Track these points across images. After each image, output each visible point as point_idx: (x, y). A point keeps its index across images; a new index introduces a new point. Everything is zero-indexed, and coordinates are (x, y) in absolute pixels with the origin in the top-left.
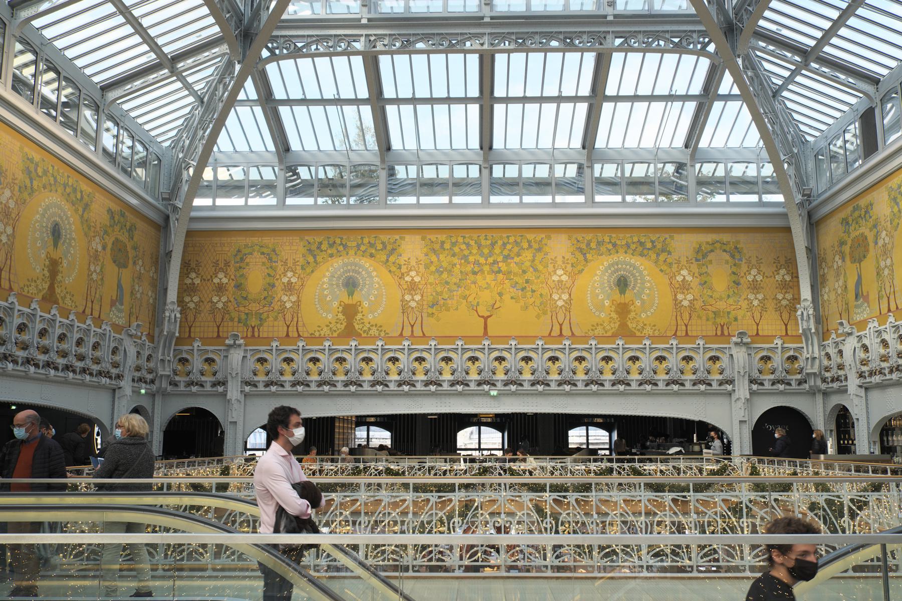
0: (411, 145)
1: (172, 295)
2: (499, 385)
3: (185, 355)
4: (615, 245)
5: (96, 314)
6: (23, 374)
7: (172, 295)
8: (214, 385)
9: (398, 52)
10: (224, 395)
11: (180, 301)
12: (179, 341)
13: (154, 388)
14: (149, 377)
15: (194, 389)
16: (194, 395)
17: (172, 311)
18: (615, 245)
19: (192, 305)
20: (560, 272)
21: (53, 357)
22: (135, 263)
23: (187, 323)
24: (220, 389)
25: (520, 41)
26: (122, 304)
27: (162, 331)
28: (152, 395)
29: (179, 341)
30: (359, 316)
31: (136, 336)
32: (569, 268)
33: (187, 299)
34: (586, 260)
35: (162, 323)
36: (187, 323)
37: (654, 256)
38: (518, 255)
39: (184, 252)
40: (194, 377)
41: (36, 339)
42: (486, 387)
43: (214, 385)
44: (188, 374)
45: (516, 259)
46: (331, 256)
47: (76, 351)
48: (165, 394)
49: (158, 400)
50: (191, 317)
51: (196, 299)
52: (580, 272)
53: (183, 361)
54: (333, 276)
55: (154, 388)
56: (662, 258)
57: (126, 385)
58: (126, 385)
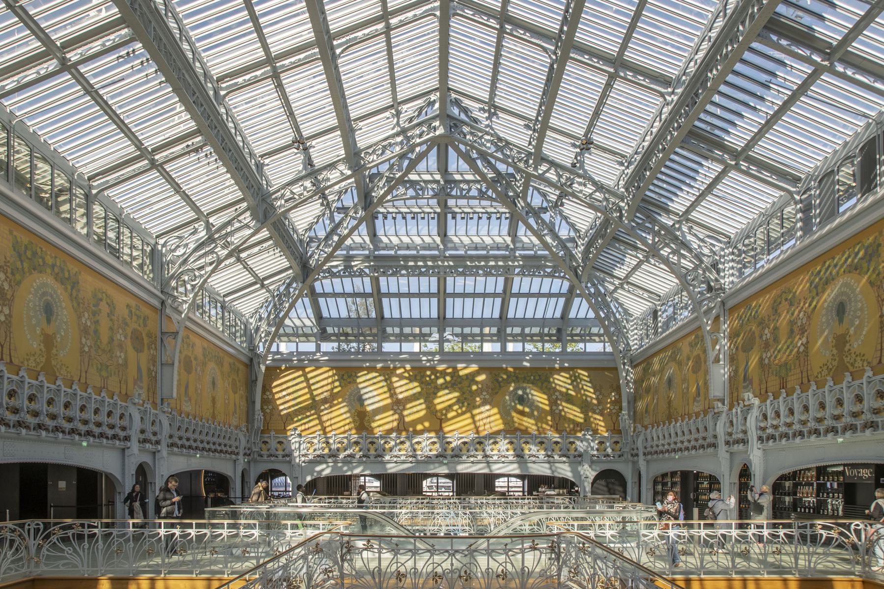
0: (396, 315)
1: (258, 406)
2: (449, 457)
3: (266, 440)
4: (517, 378)
5: (83, 381)
6: (36, 437)
7: (258, 406)
8: (283, 456)
9: (391, 275)
10: (290, 462)
11: (262, 408)
12: (263, 432)
13: (250, 458)
14: (248, 452)
15: (273, 459)
16: (272, 462)
17: (259, 415)
18: (517, 378)
19: (268, 411)
20: (484, 393)
21: (105, 429)
22: (149, 349)
23: (267, 423)
24: (288, 459)
25: (461, 270)
26: (142, 382)
27: (253, 426)
28: (249, 462)
29: (263, 432)
30: (367, 418)
31: (167, 412)
32: (490, 391)
33: (265, 407)
34: (500, 386)
35: (253, 422)
36: (267, 423)
37: (540, 384)
38: (460, 383)
39: (264, 380)
40: (272, 452)
41: (26, 402)
42: (441, 459)
43: (283, 456)
44: (268, 450)
45: (459, 386)
46: (350, 383)
47: (47, 411)
48: (255, 461)
49: (252, 465)
50: (268, 418)
51: (270, 407)
52: (496, 393)
53: (265, 443)
54: (351, 395)
55: (250, 458)
56: (545, 385)
57: (241, 457)
58: (241, 457)
